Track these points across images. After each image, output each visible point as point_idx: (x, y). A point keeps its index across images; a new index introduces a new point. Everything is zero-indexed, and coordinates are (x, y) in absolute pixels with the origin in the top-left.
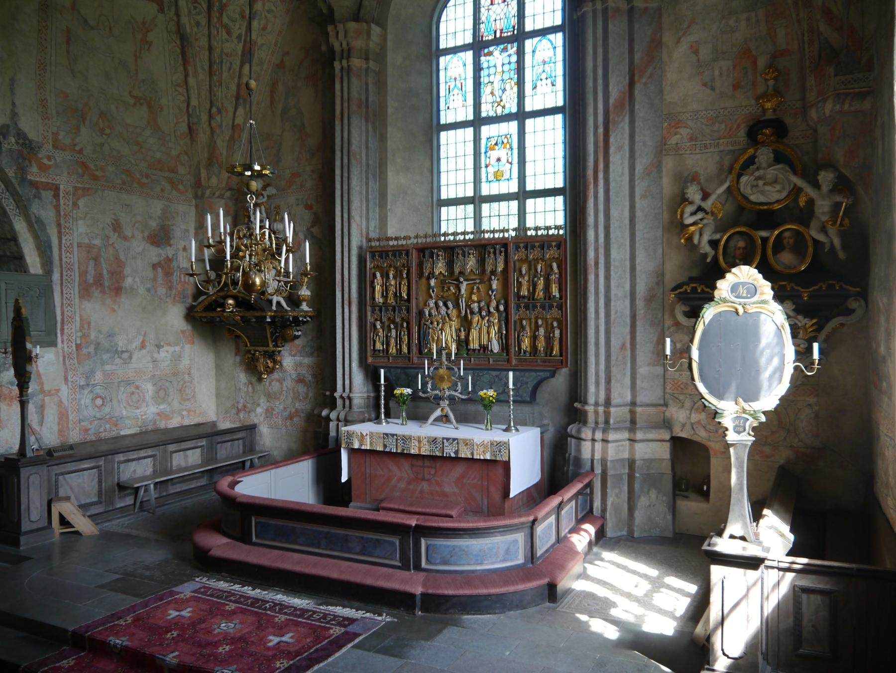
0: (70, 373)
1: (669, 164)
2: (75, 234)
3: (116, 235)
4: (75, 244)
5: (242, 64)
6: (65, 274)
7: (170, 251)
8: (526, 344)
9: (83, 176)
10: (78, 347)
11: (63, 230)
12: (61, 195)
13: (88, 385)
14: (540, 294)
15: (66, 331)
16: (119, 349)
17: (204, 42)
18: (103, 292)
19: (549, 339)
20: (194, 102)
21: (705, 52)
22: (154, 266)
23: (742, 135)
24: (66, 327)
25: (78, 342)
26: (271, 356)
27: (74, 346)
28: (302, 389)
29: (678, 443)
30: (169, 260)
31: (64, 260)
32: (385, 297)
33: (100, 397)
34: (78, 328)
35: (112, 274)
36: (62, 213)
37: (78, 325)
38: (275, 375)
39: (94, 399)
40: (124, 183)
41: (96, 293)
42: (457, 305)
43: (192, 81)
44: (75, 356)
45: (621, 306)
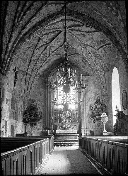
1: (89, 103)
5: (32, 84)
8: (74, 121)
14: (76, 116)
17: (28, 81)
19: (77, 121)
21: (92, 92)
23: (96, 100)
26: (36, 124)
28: (40, 128)
29: (91, 131)
32: (56, 116)
38: (35, 126)
42: (66, 117)
43: (26, 86)
45: (85, 117)
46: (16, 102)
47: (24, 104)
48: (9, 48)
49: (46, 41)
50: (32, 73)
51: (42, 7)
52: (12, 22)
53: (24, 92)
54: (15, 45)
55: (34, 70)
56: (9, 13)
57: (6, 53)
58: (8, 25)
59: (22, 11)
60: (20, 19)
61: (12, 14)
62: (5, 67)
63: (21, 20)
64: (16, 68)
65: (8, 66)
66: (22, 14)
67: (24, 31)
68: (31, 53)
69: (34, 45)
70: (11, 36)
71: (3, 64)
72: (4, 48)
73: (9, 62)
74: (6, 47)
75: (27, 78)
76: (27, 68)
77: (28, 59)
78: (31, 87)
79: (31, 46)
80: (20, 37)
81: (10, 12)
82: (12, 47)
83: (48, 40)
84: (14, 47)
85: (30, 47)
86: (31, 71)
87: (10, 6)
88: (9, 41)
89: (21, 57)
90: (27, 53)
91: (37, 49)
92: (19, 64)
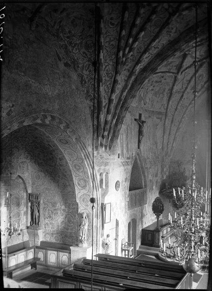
17: (169, 128)
20: (165, 141)
43: (165, 137)
46: (143, 173)
47: (162, 170)
48: (114, 102)
49: (200, 56)
50: (176, 113)
51: (169, 19)
52: (114, 57)
53: (163, 148)
54: (125, 94)
55: (179, 107)
56: (107, 45)
57: (108, 112)
58: (106, 64)
59: (130, 35)
60: (127, 49)
61: (112, 45)
62: (108, 135)
63: (129, 52)
64: (140, 115)
65: (114, 132)
66: (131, 40)
67: (139, 68)
68: (170, 81)
69: (175, 66)
70: (115, 82)
71: (104, 131)
72: (104, 104)
73: (116, 125)
74: (107, 101)
75: (166, 123)
76: (166, 105)
77: (166, 91)
78: (175, 137)
79: (170, 69)
80: (133, 78)
81: (107, 42)
82: (120, 99)
83: (203, 54)
84: (123, 98)
85: (167, 70)
86: (174, 110)
87: (106, 33)
88: (113, 91)
89: (152, 90)
90: (163, 81)
91: (181, 74)
92: (150, 103)
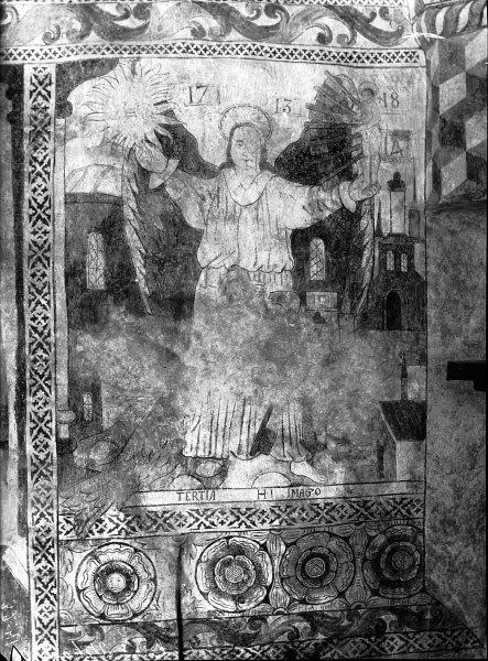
0: (30, 511)
2: (59, 176)
3: (174, 163)
4: (60, 198)
6: (27, 272)
7: (349, 195)
9: (82, 37)
10: (65, 447)
11: (27, 169)
12: (27, 87)
13: (83, 541)
15: (30, 408)
16: (188, 453)
18: (137, 310)
22: (299, 239)
24: (30, 399)
25: (64, 435)
27: (52, 442)
30: (349, 217)
31: (28, 237)
33: (119, 570)
34: (64, 400)
35: (161, 264)
36: (27, 129)
37: (64, 391)
39: (102, 576)
40: (198, 33)
41: (118, 315)
44: (54, 469)
